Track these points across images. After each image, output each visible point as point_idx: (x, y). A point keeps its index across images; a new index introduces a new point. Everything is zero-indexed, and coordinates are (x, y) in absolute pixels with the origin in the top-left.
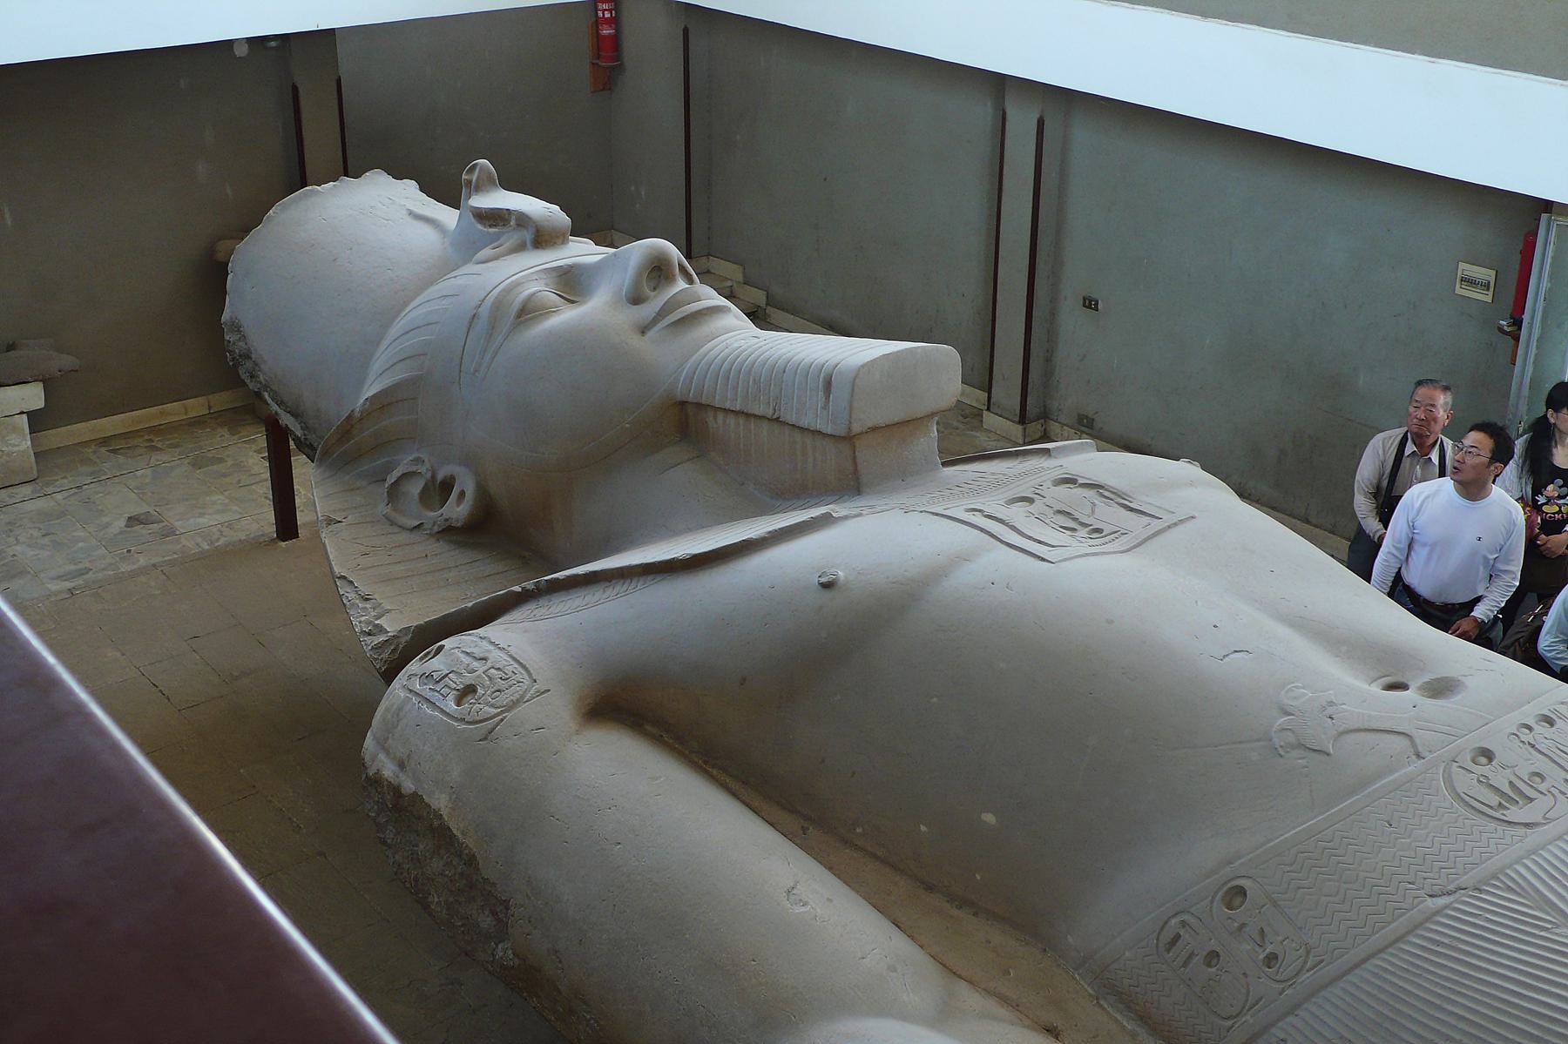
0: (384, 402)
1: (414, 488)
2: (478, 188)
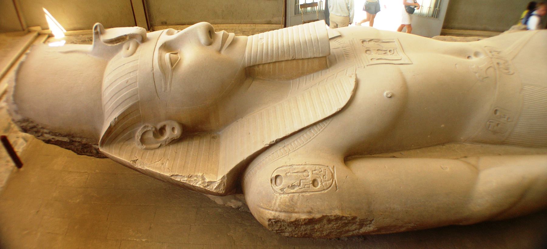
0: (123, 117)
1: (150, 135)
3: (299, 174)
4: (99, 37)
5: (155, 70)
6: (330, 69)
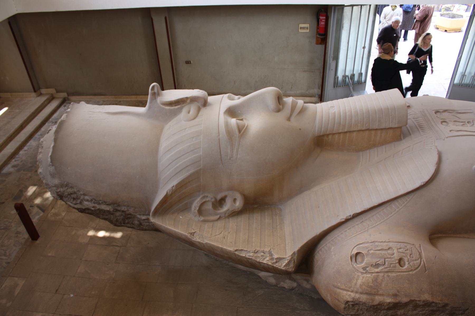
0: (181, 185)
1: (209, 206)
2: (155, 95)
3: (383, 252)
4: (155, 99)
5: (221, 136)
6: (404, 141)
